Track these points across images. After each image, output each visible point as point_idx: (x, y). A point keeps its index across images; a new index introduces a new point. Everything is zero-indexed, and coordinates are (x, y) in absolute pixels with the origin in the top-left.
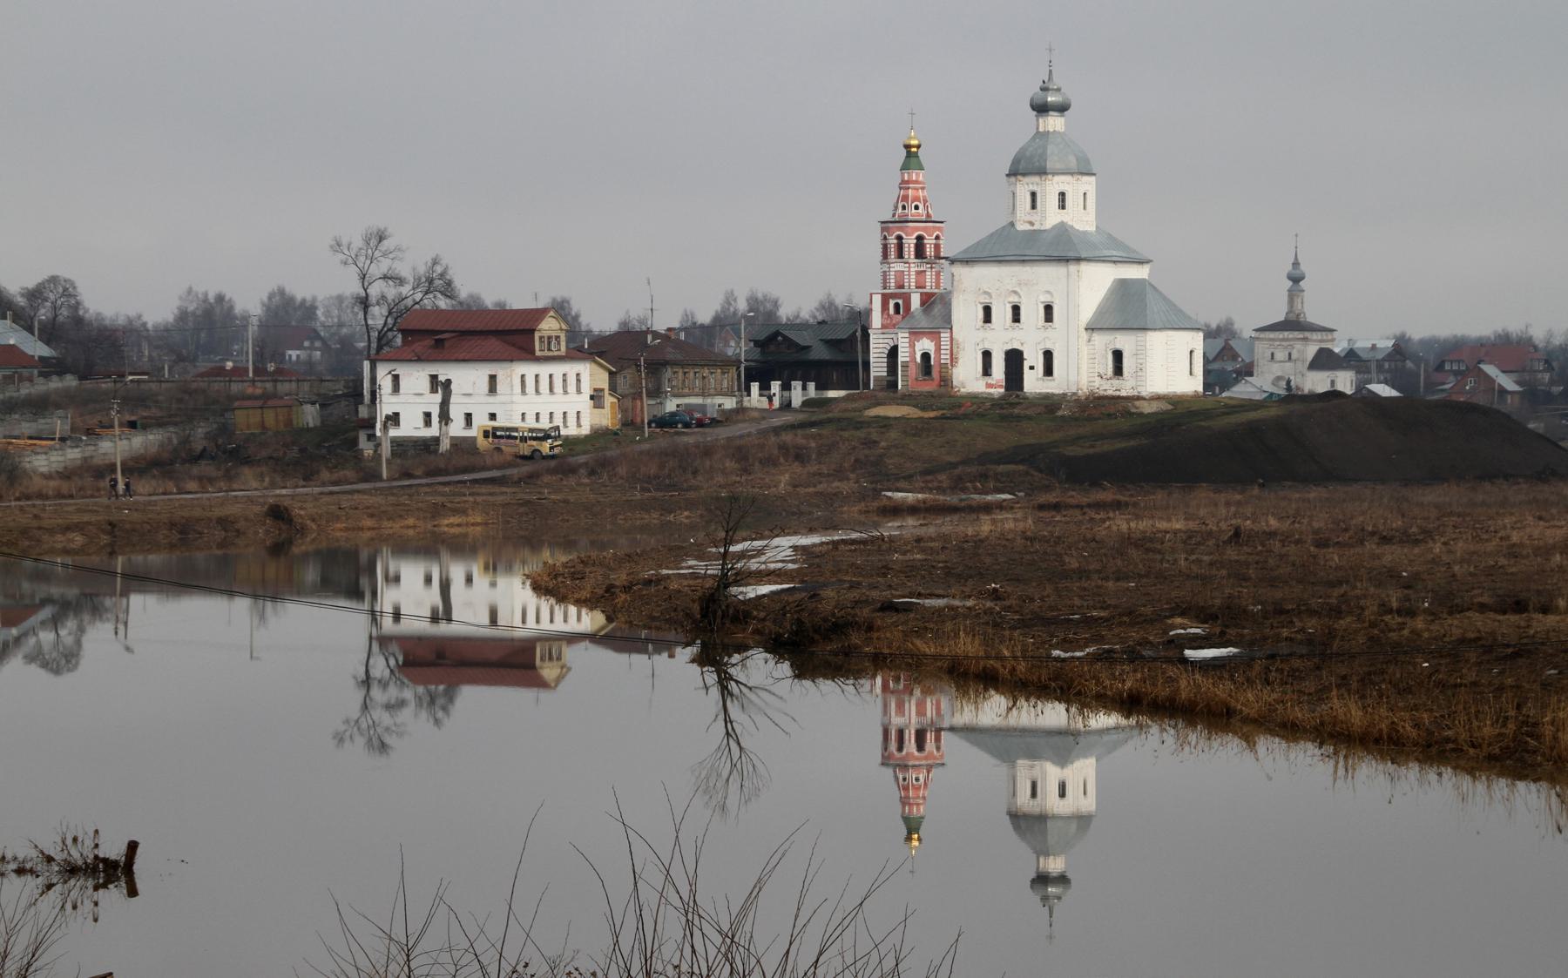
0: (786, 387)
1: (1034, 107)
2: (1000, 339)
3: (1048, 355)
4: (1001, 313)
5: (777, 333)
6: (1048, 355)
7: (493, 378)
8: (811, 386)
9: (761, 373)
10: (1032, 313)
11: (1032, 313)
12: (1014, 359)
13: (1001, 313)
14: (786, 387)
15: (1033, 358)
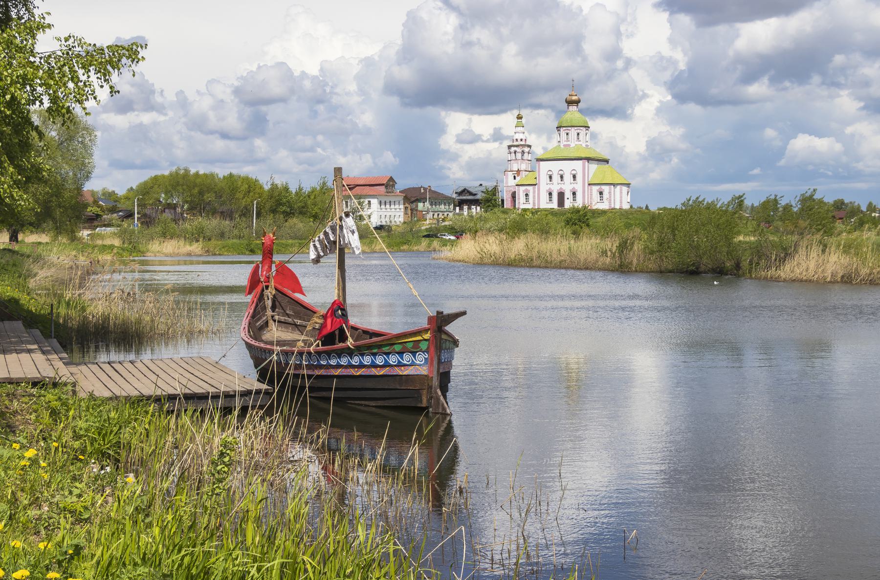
0: (469, 208)
1: (566, 101)
2: (555, 189)
3: (574, 194)
4: (556, 178)
5: (465, 190)
6: (574, 194)
7: (369, 202)
8: (478, 208)
9: (461, 204)
10: (568, 178)
11: (568, 178)
12: (561, 195)
13: (556, 178)
14: (469, 208)
15: (568, 195)
